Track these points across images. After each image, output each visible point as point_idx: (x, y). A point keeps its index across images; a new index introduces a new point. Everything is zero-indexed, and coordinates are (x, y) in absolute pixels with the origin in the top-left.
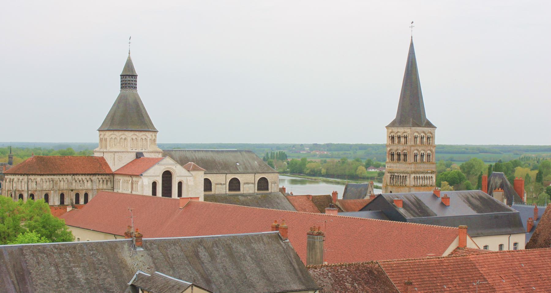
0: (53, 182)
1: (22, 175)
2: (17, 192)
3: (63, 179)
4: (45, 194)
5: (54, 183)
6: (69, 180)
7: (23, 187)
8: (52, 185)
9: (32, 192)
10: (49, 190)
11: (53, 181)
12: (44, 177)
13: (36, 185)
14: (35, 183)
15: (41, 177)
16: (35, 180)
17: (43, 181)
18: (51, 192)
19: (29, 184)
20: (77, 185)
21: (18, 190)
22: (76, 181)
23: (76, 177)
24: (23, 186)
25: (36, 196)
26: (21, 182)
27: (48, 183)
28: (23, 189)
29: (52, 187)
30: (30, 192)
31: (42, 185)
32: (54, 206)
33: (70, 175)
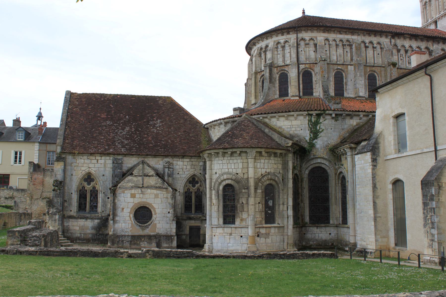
0: (351, 48)
1: (285, 34)
2: (275, 70)
3: (371, 42)
4: (334, 72)
5: (354, 49)
6: (386, 46)
7: (286, 59)
8: (349, 55)
9: (307, 66)
10: (343, 65)
11: (351, 46)
12: (332, 36)
13: (315, 51)
14: (312, 48)
15: (326, 35)
16: (312, 43)
17: (329, 45)
18: (347, 68)
19: (300, 50)
20: (401, 59)
21: (276, 65)
22: (399, 51)
23: (399, 42)
24: (287, 55)
25: (315, 75)
26: (283, 47)
27: (340, 50)
28: (288, 62)
29: (349, 59)
30: (302, 67)
31: (328, 52)
32: (357, 98)
33: (387, 37)
